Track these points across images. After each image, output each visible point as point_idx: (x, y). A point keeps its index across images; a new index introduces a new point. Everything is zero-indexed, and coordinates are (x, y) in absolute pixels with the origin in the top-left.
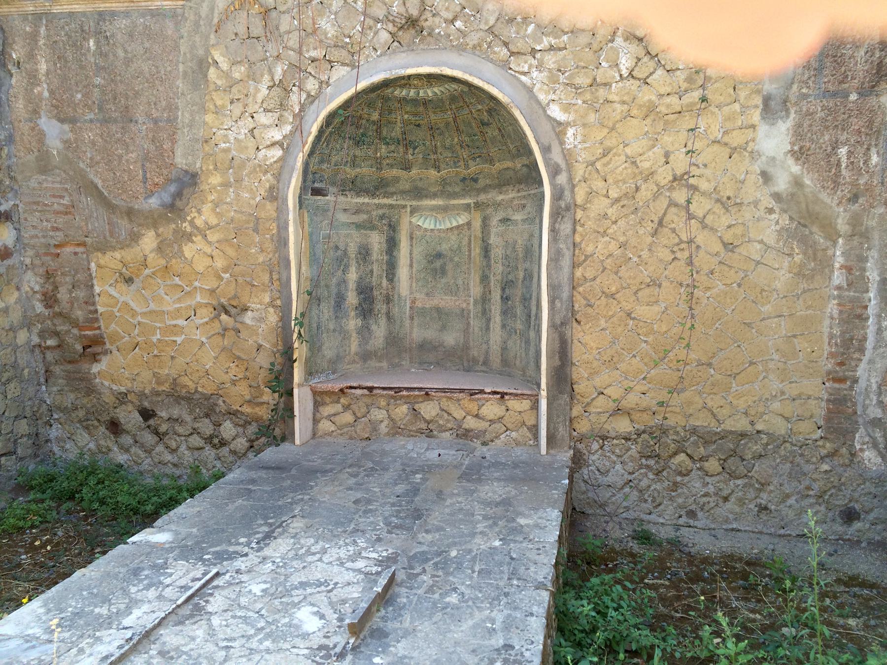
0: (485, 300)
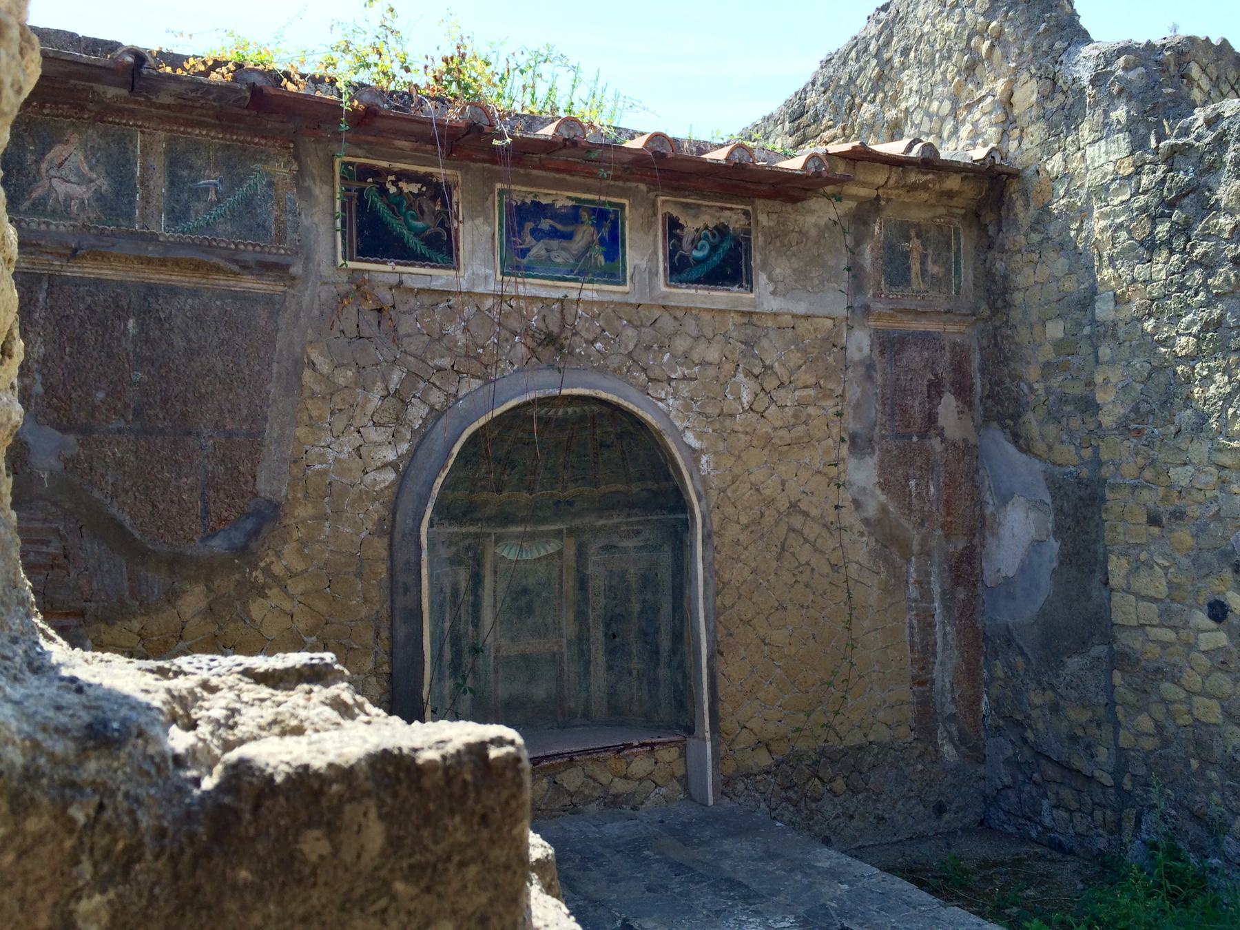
0: (582, 639)
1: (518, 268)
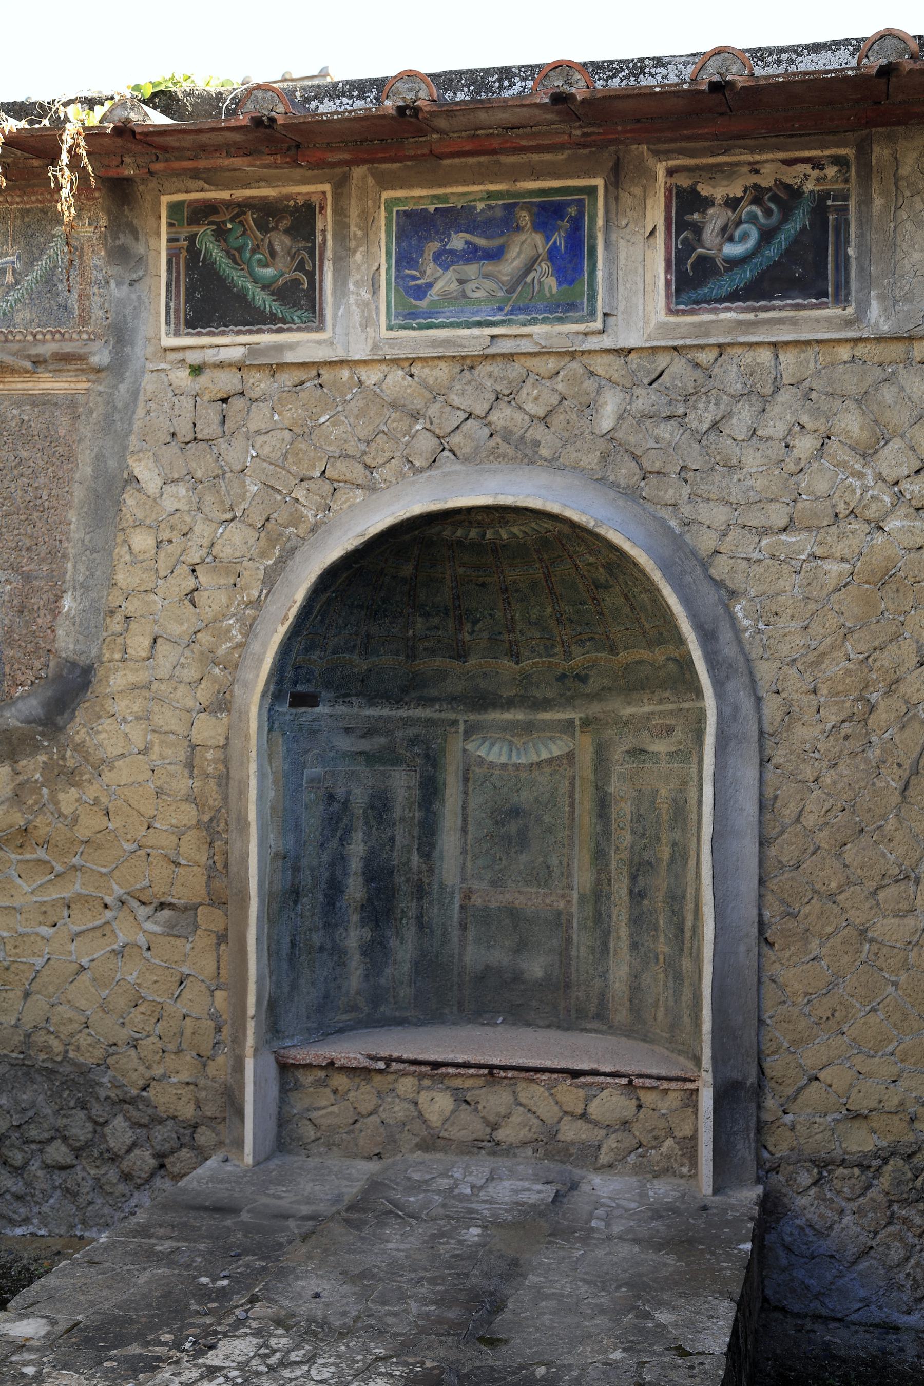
1: (413, 315)
